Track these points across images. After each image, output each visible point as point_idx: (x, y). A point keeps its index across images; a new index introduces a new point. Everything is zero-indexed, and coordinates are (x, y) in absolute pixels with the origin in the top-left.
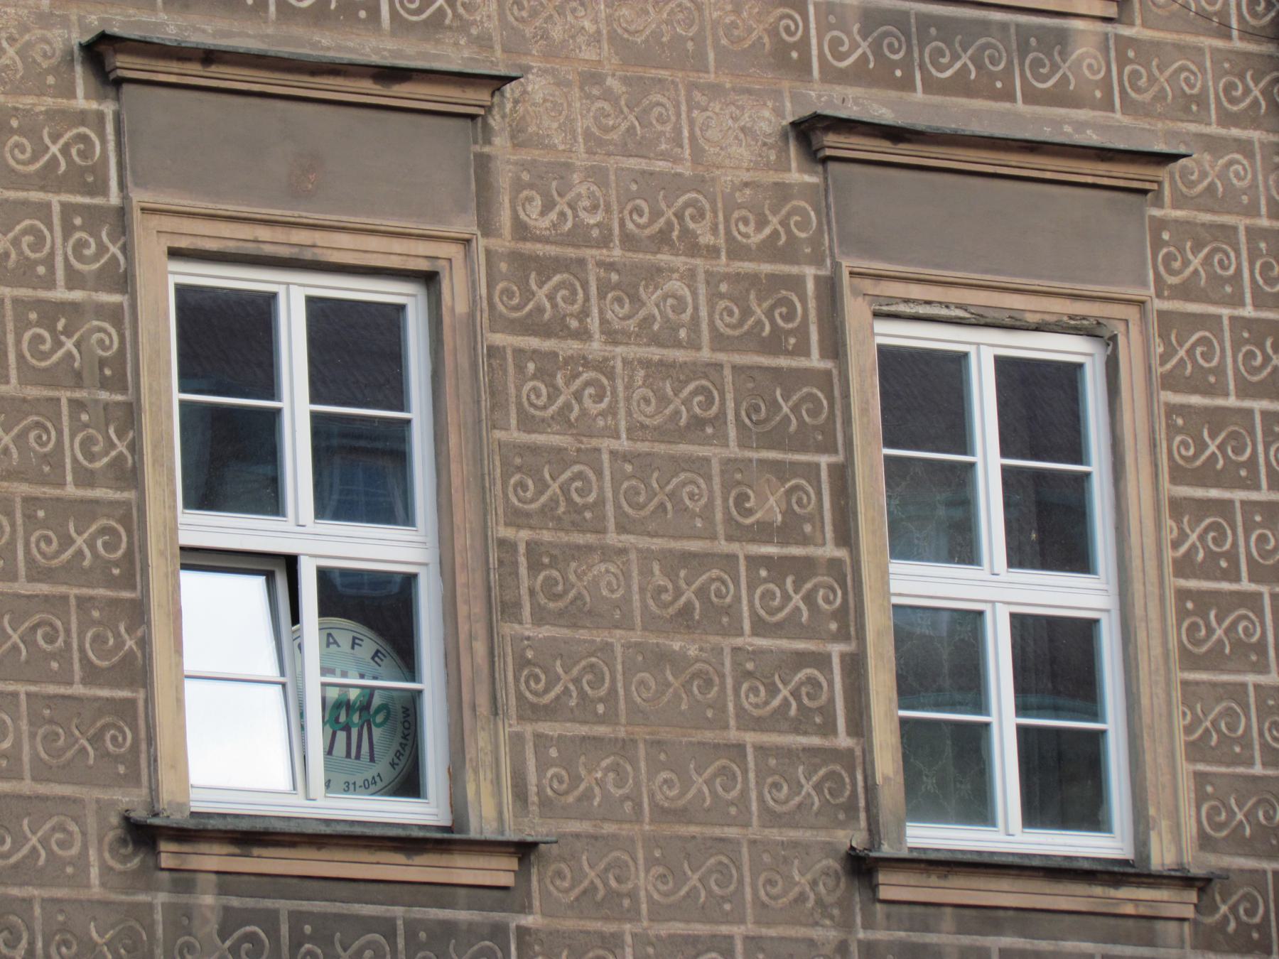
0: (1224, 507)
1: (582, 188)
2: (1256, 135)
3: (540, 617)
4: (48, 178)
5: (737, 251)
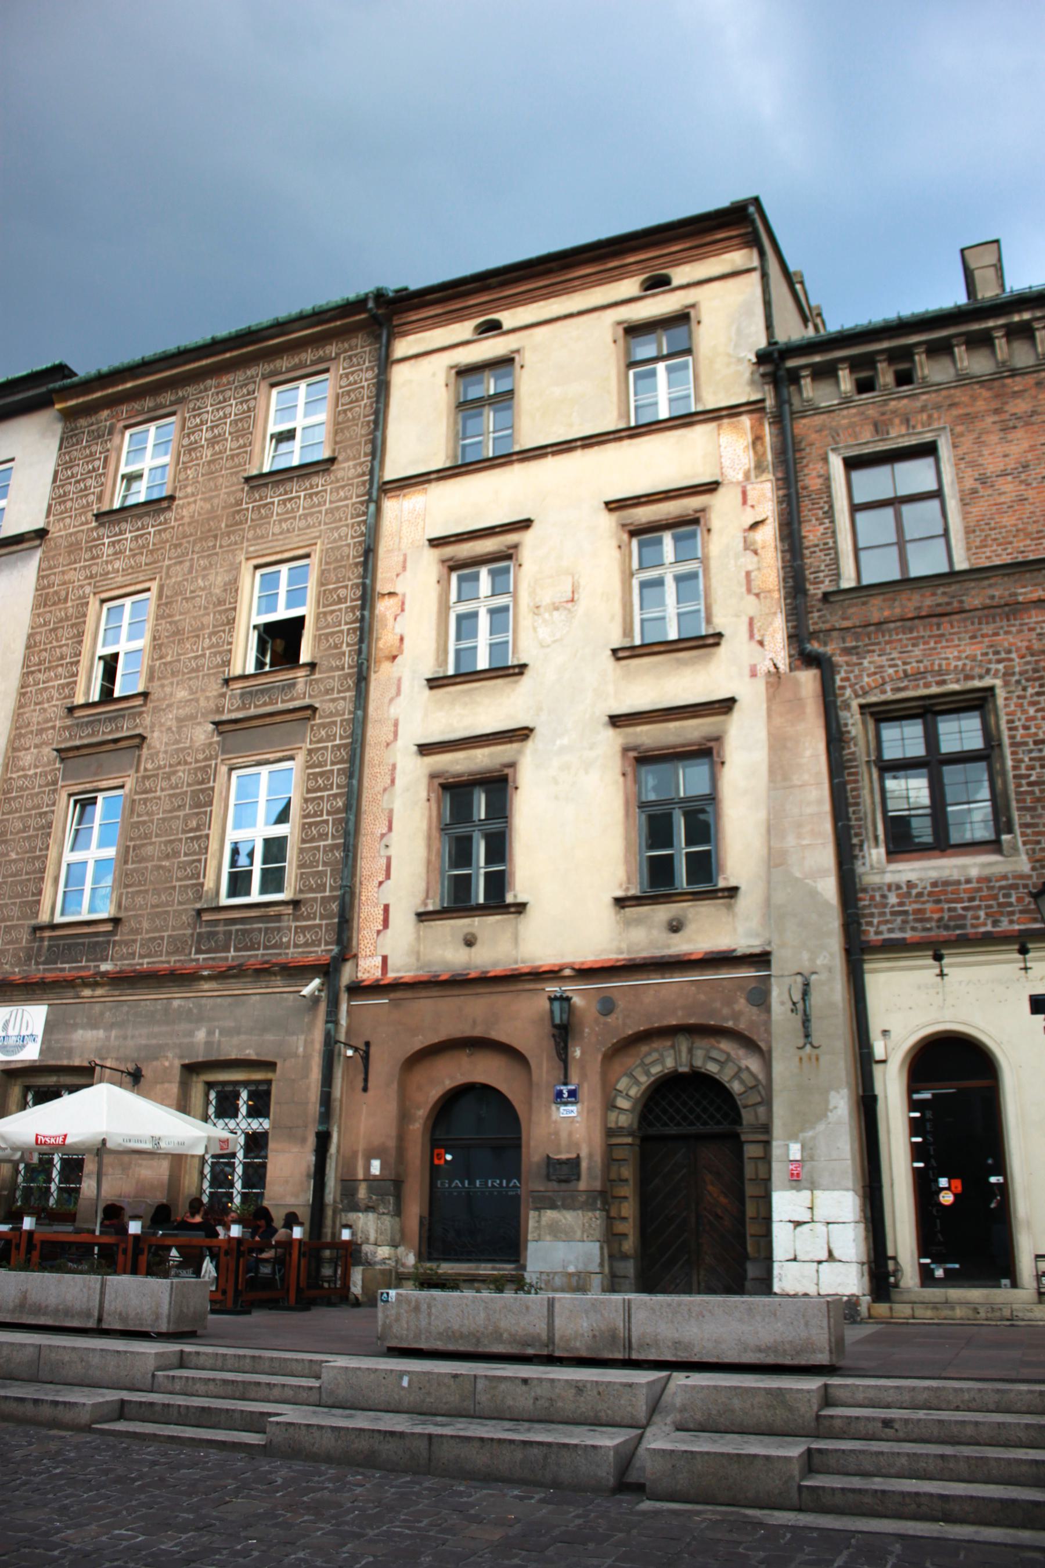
0: (321, 798)
1: (161, 756)
2: (348, 694)
3: (133, 862)
4: (48, 785)
5: (197, 761)
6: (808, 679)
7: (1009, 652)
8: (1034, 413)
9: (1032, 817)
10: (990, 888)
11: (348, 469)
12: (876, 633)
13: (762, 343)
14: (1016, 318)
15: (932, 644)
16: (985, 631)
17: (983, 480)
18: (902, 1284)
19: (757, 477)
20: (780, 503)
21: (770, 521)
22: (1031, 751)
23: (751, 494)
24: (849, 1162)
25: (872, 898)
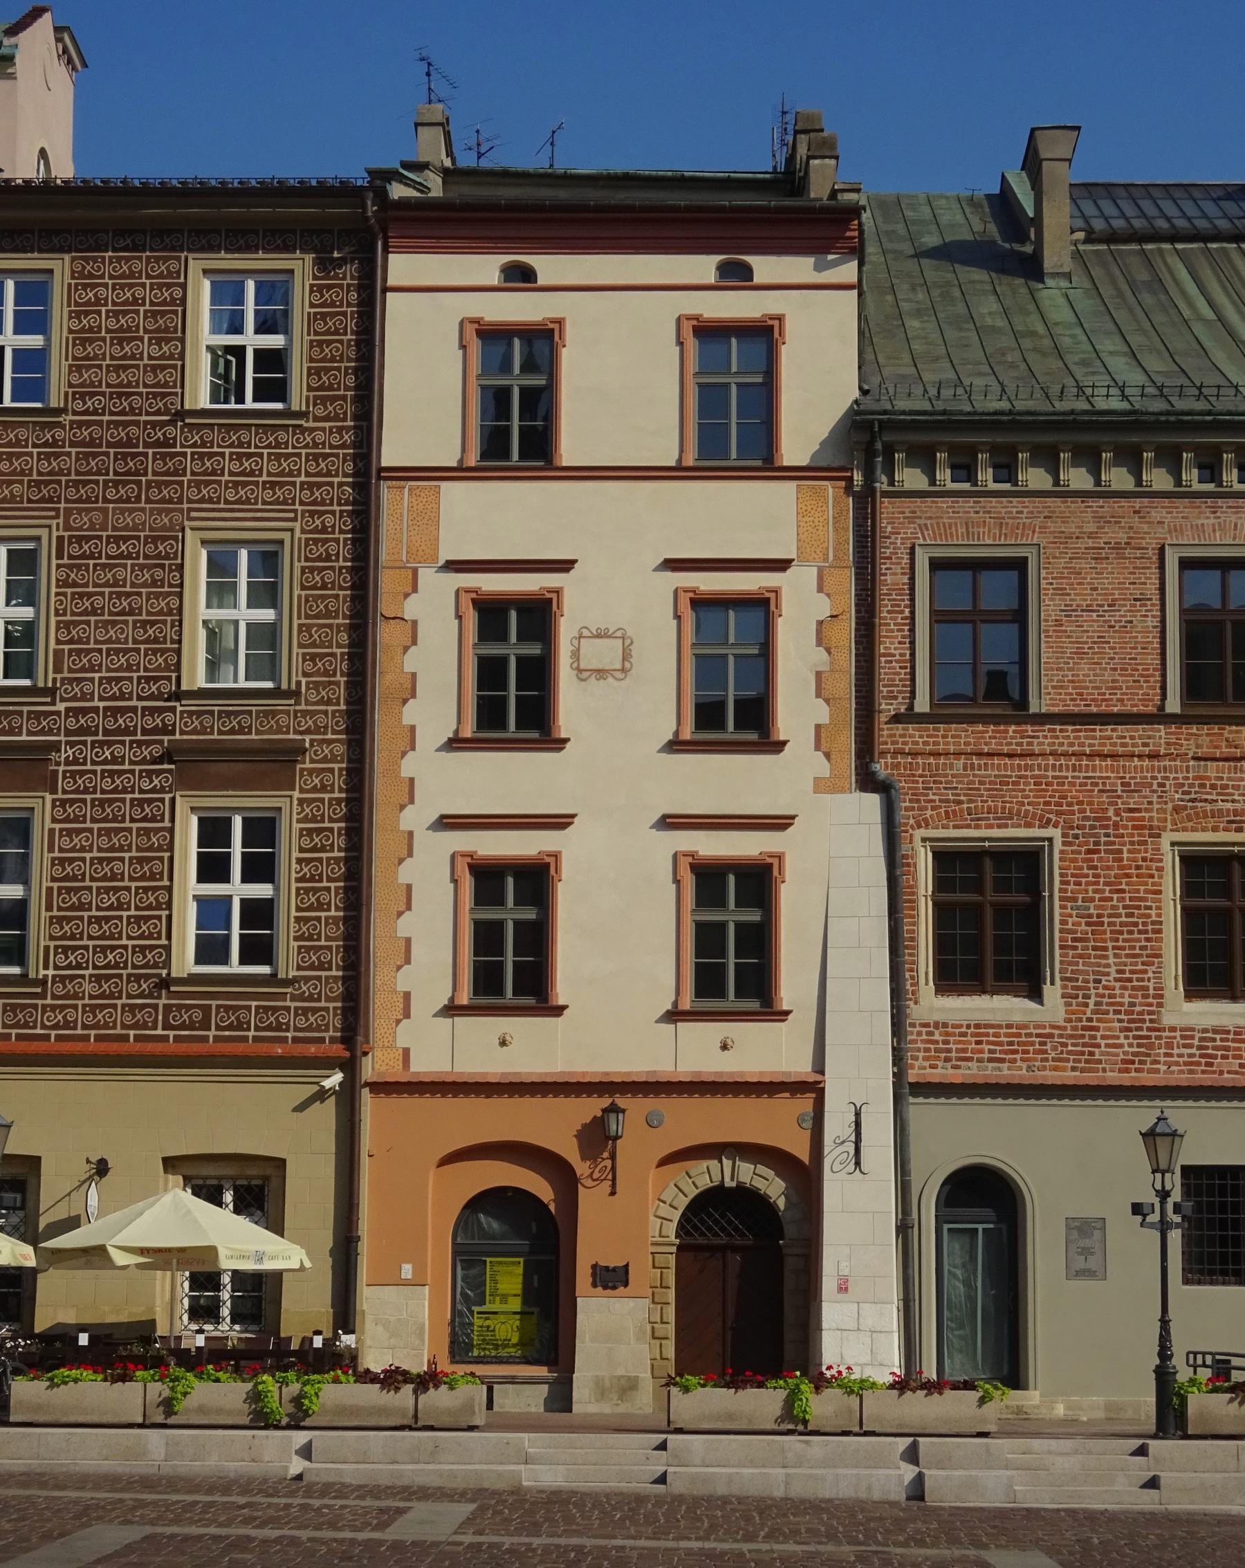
11: (332, 435)
23: (828, 580)
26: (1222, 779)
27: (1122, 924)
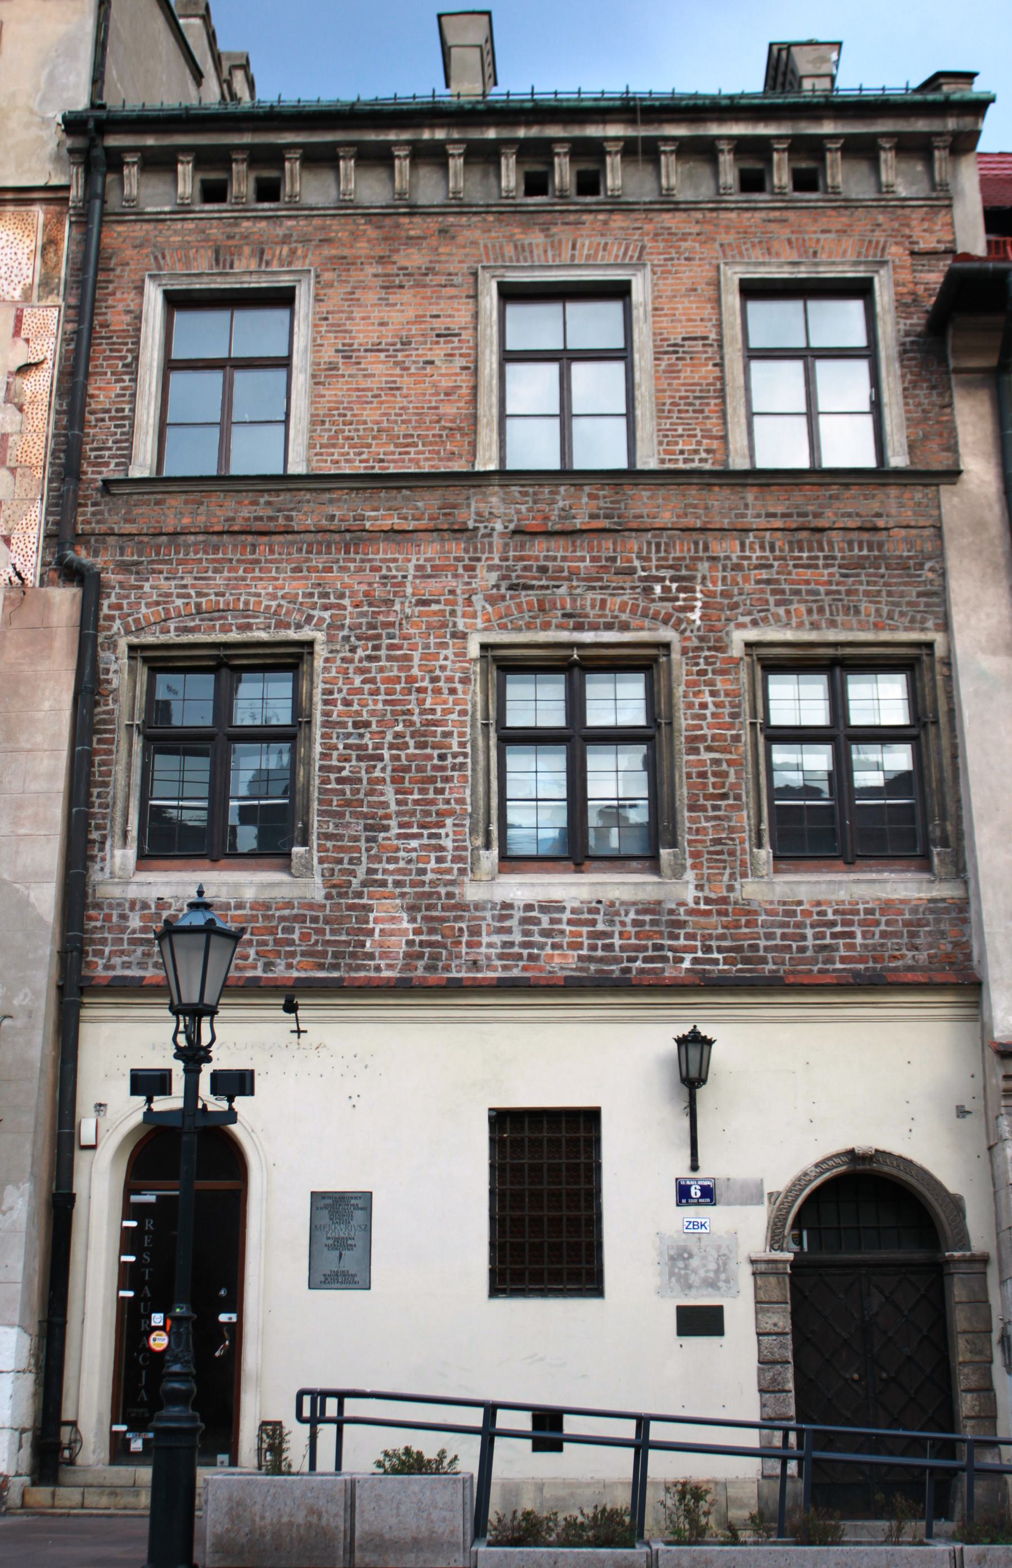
6: (64, 600)
7: (342, 596)
8: (430, 271)
9: (336, 826)
10: (266, 917)
12: (168, 546)
13: (81, 102)
14: (426, 135)
15: (241, 573)
16: (314, 563)
17: (347, 353)
18: (80, 1460)
19: (40, 299)
20: (66, 341)
21: (48, 365)
22: (348, 735)
24: (19, 1286)
25: (108, 918)
26: (555, 559)
27: (410, 758)
